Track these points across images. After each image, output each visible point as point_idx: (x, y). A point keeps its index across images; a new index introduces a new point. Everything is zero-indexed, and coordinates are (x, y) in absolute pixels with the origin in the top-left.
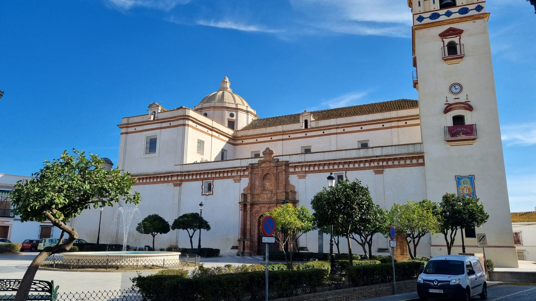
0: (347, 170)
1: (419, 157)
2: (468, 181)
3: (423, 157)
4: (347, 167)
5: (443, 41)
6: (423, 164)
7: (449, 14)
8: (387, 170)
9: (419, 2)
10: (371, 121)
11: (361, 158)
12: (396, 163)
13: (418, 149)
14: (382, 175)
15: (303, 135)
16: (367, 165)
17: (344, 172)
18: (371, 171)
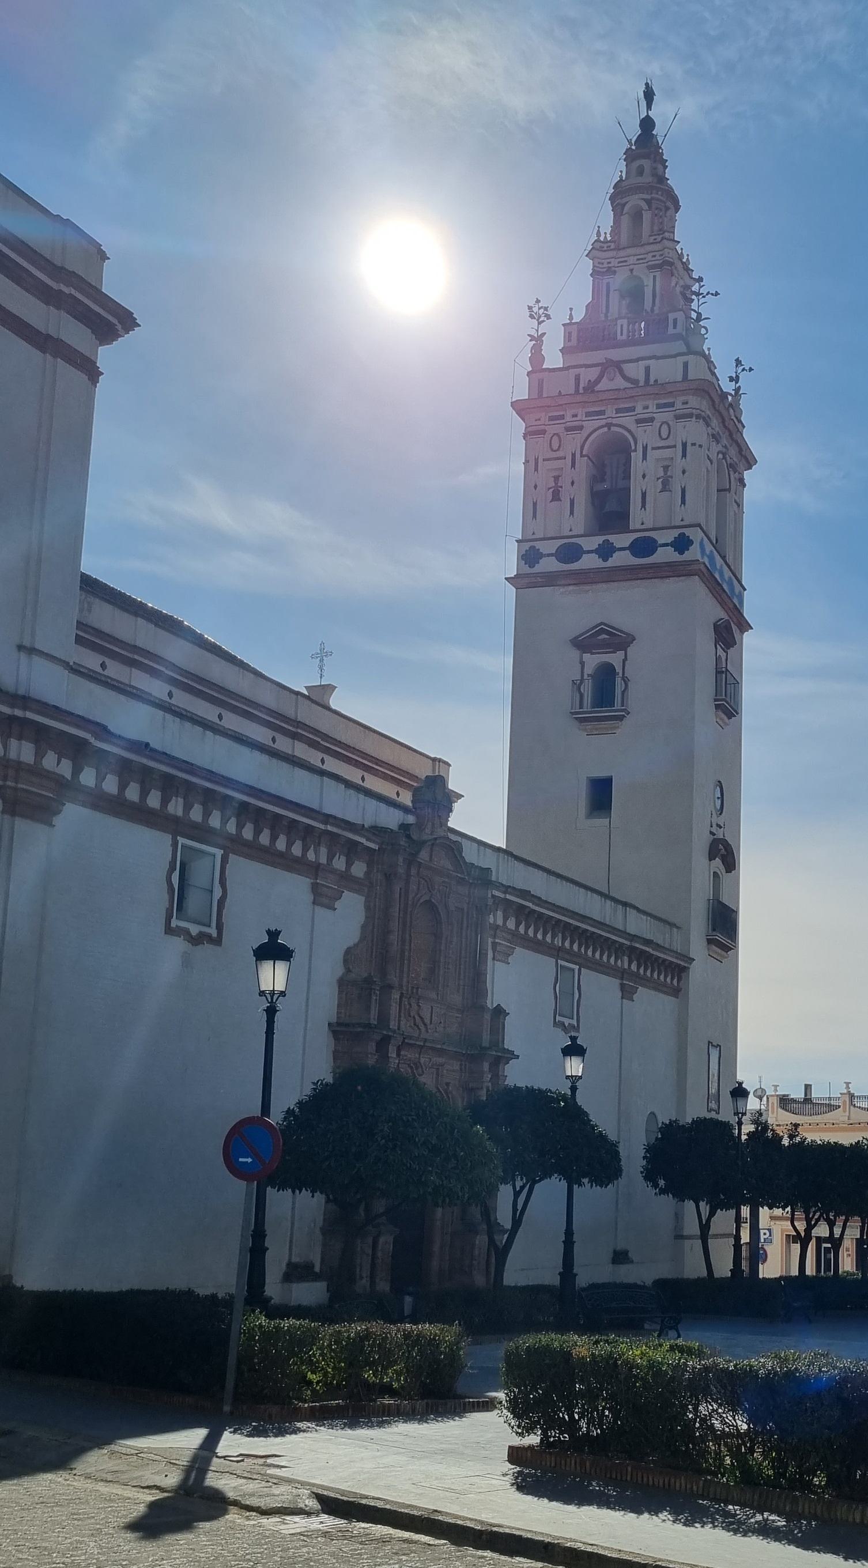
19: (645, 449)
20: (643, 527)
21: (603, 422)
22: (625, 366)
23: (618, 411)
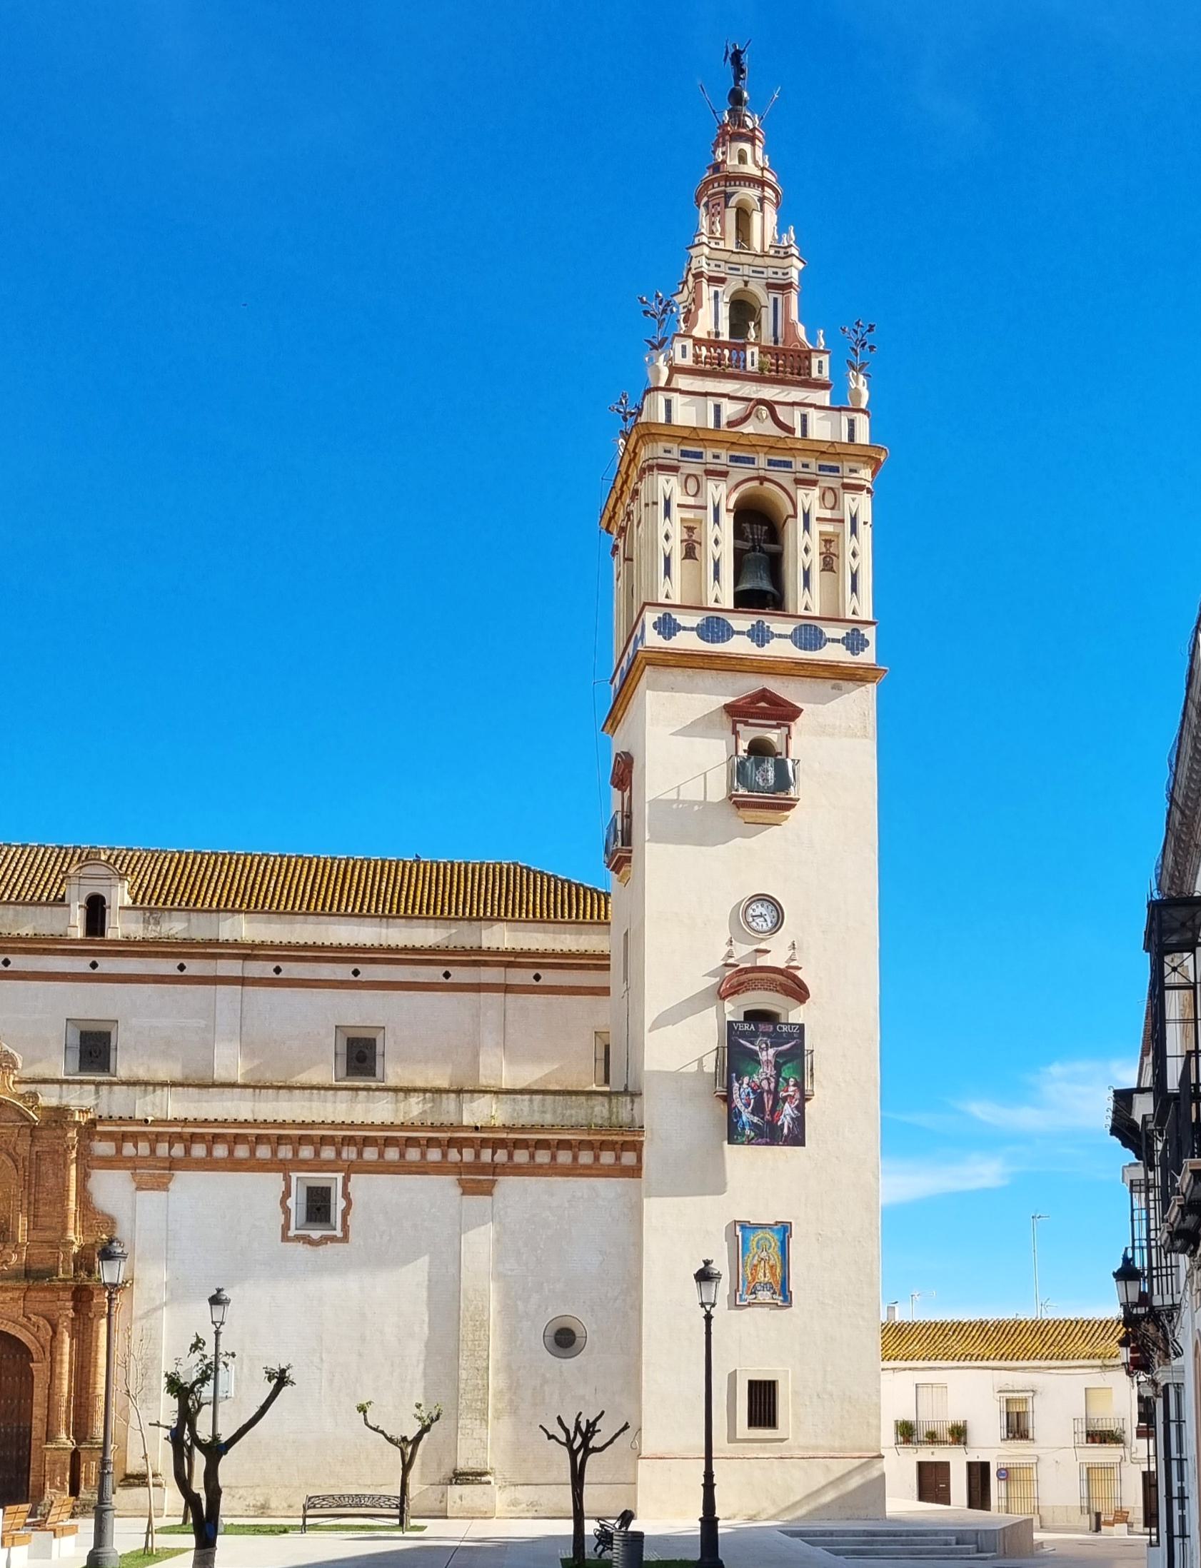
0: (350, 1169)
1: (625, 1146)
2: (773, 1239)
3: (637, 1147)
4: (354, 1156)
5: (736, 733)
6: (635, 1171)
7: (760, 635)
8: (507, 1184)
9: (667, 560)
10: (397, 950)
11: (413, 1127)
12: (543, 1157)
13: (623, 1111)
14: (488, 1198)
15: (82, 965)
16: (434, 1155)
17: (340, 1176)
18: (445, 1186)
19: (806, 516)
20: (855, 617)
21: (754, 473)
22: (777, 408)
23: (770, 463)
